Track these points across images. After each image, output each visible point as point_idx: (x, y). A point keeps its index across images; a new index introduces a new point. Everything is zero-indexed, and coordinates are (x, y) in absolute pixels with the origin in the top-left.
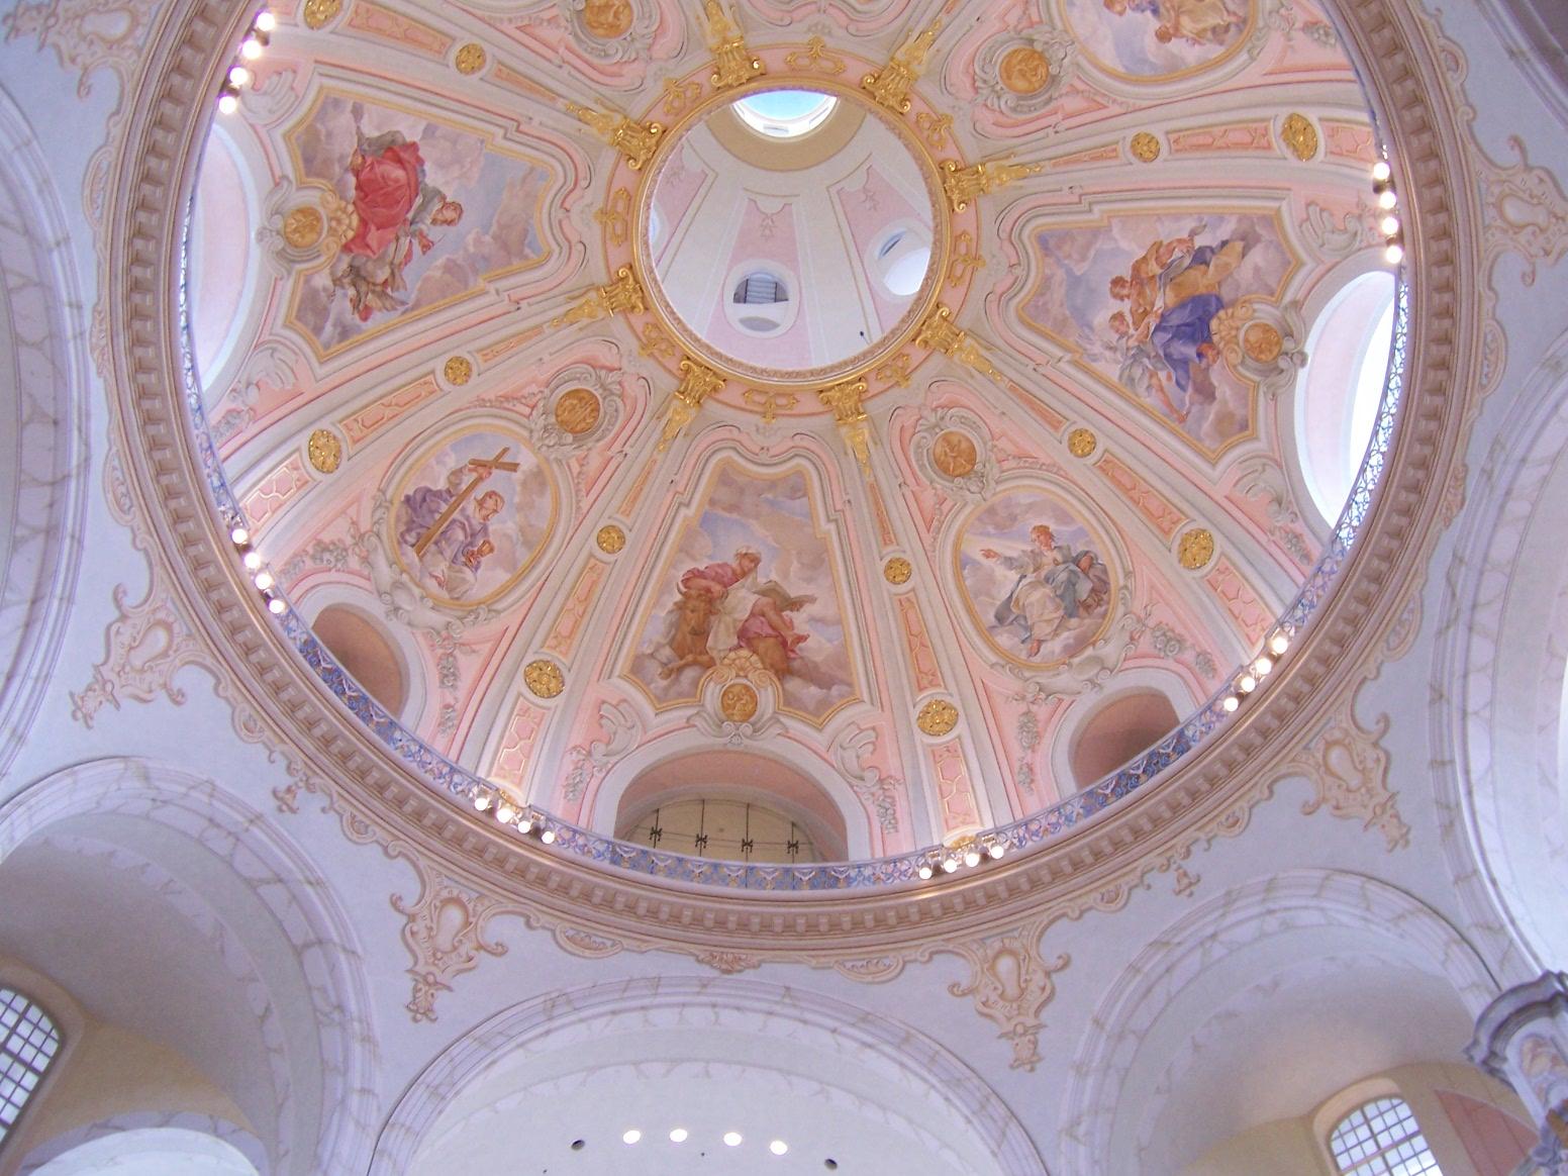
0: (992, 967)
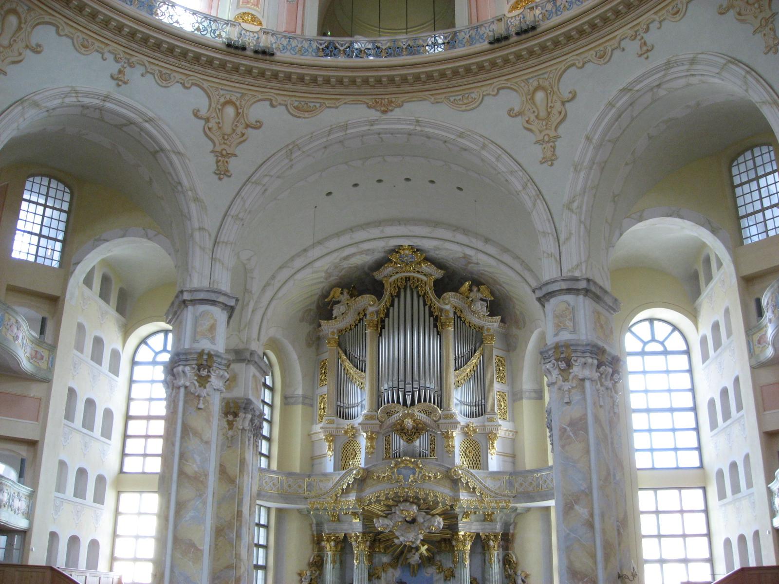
0: (532, 98)
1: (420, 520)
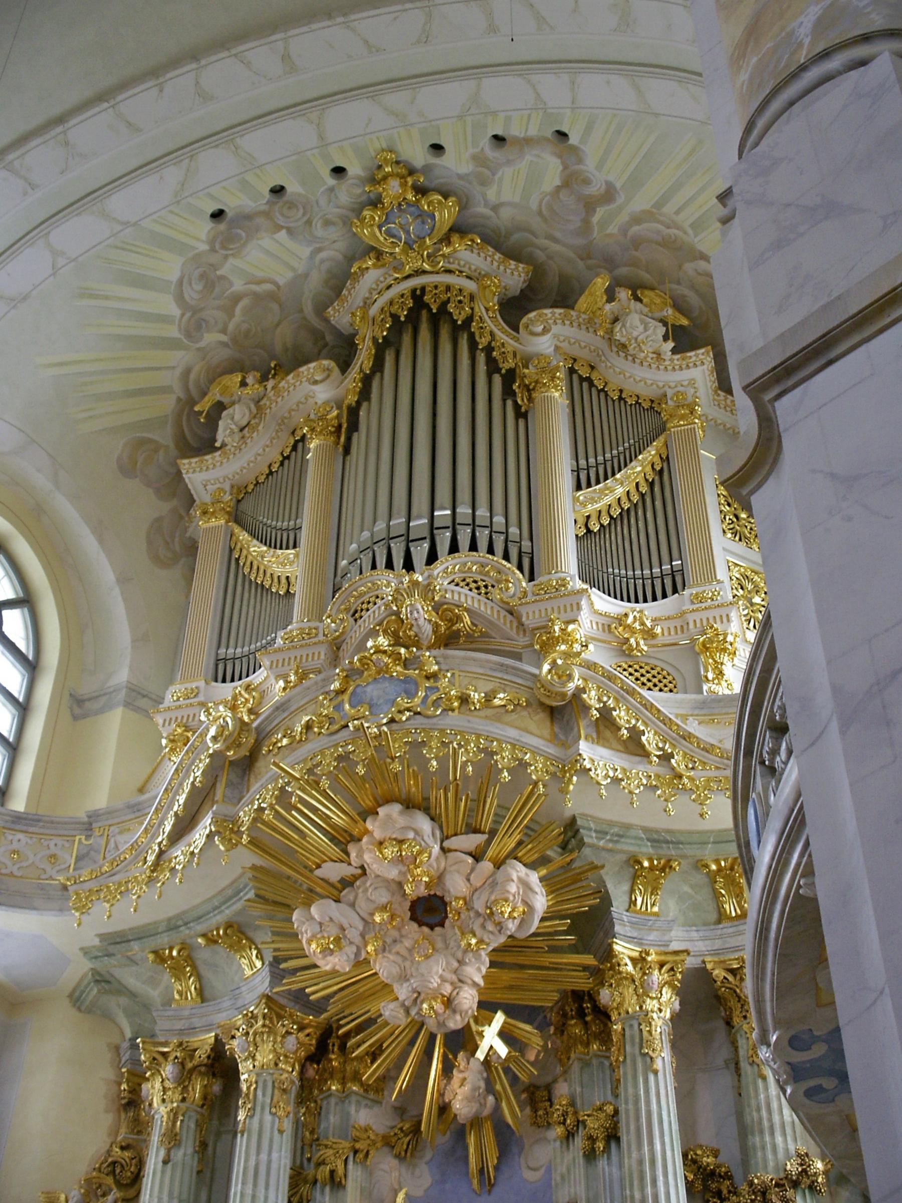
1: (456, 887)
